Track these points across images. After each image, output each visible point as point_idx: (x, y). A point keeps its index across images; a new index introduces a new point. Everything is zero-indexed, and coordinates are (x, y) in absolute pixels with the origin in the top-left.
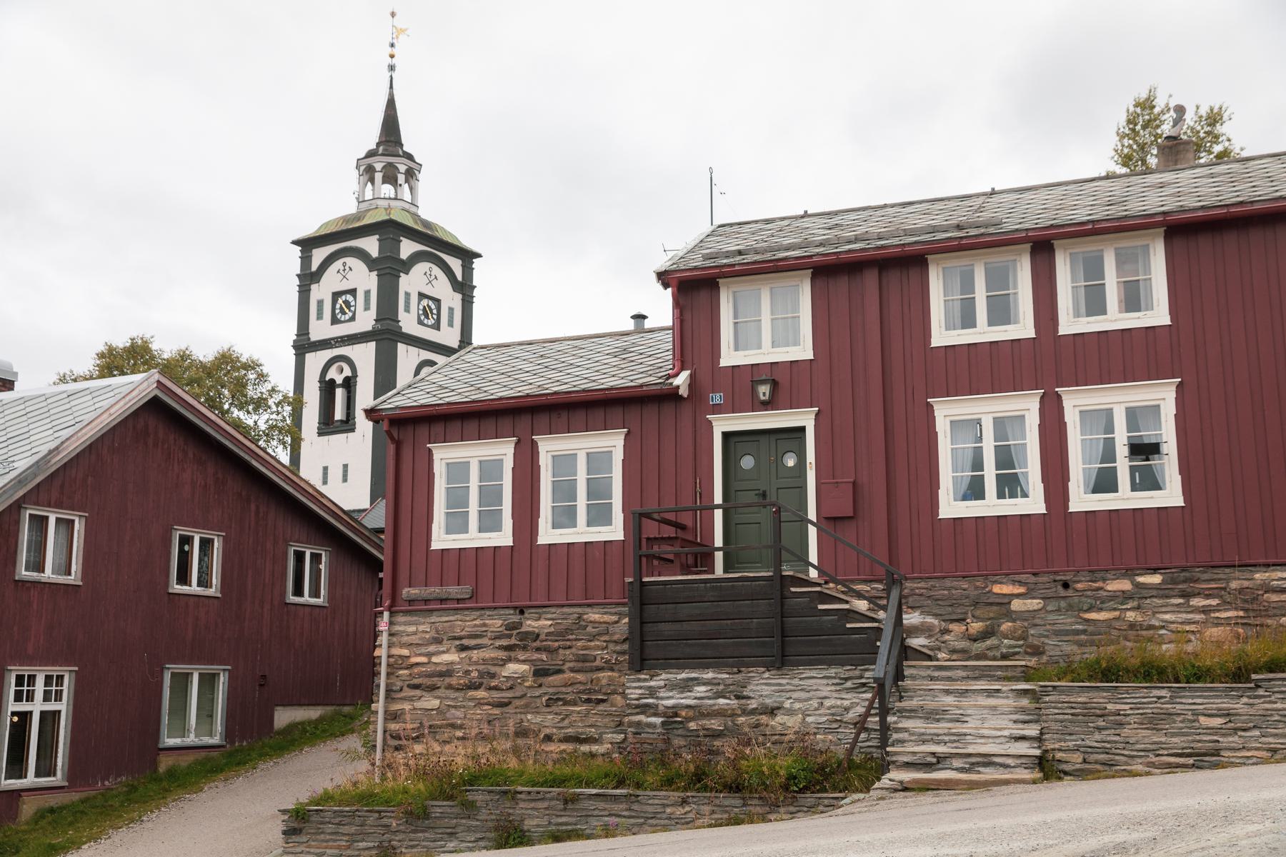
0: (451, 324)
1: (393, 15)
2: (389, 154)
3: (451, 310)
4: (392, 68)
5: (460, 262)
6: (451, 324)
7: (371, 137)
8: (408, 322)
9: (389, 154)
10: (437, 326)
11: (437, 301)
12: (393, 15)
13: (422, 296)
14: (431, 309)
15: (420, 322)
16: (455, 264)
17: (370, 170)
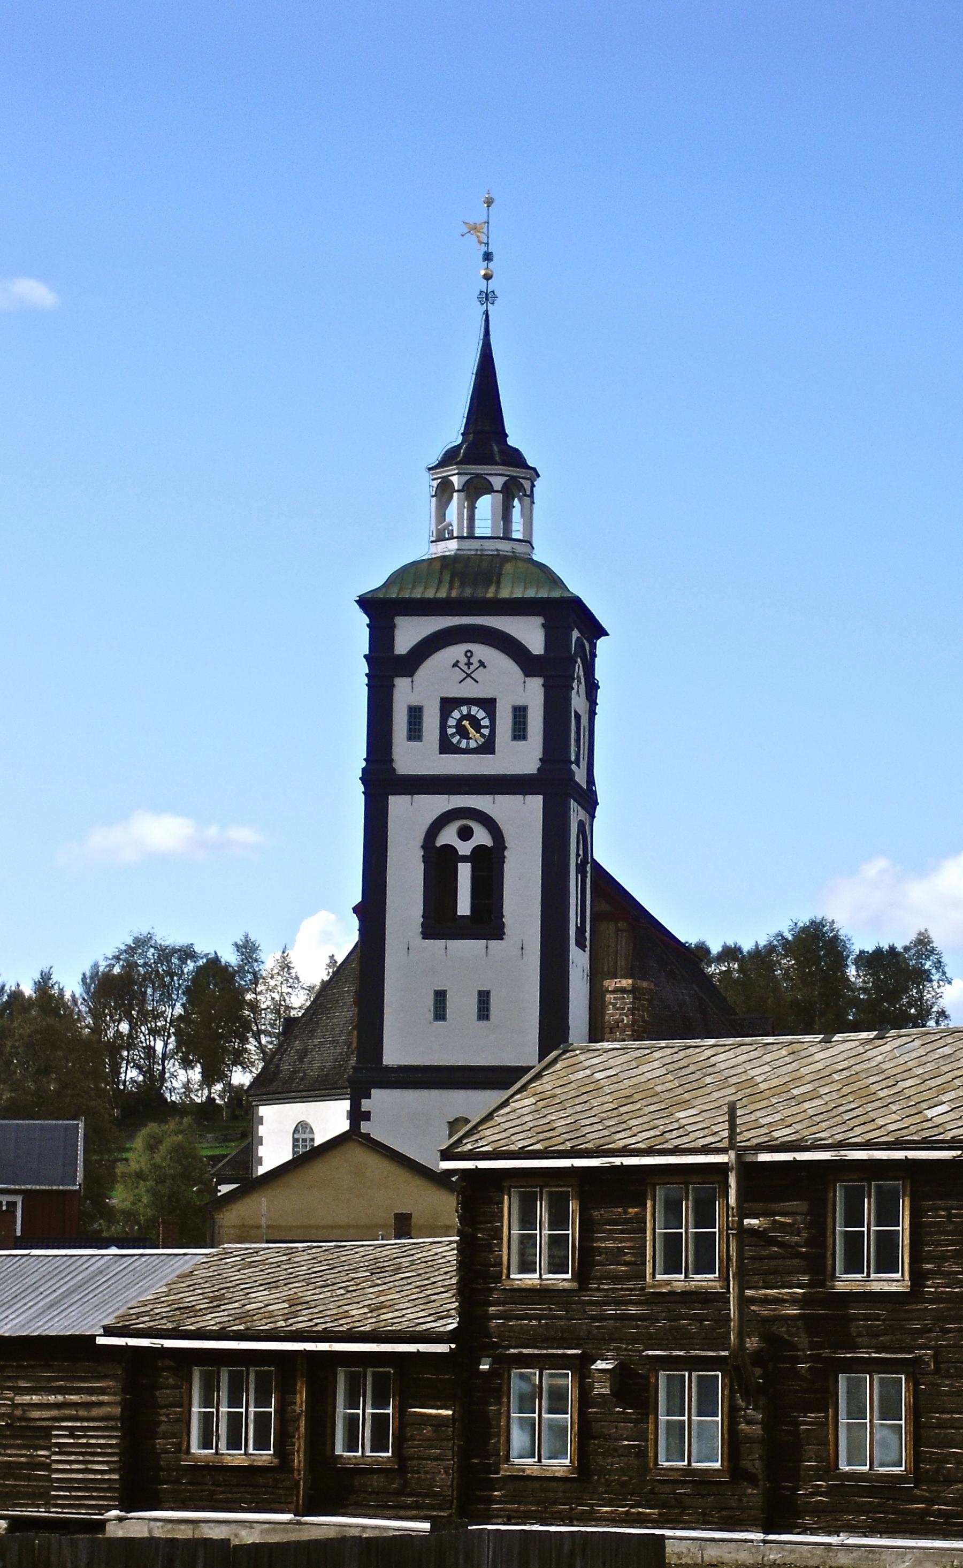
0: (520, 732)
1: (489, 202)
2: (485, 451)
3: (520, 714)
4: (487, 297)
5: (539, 620)
6: (520, 732)
7: (452, 432)
8: (412, 758)
9: (485, 451)
10: (488, 747)
11: (489, 705)
12: (489, 202)
13: (448, 705)
14: (467, 720)
15: (446, 747)
16: (531, 634)
17: (444, 491)
